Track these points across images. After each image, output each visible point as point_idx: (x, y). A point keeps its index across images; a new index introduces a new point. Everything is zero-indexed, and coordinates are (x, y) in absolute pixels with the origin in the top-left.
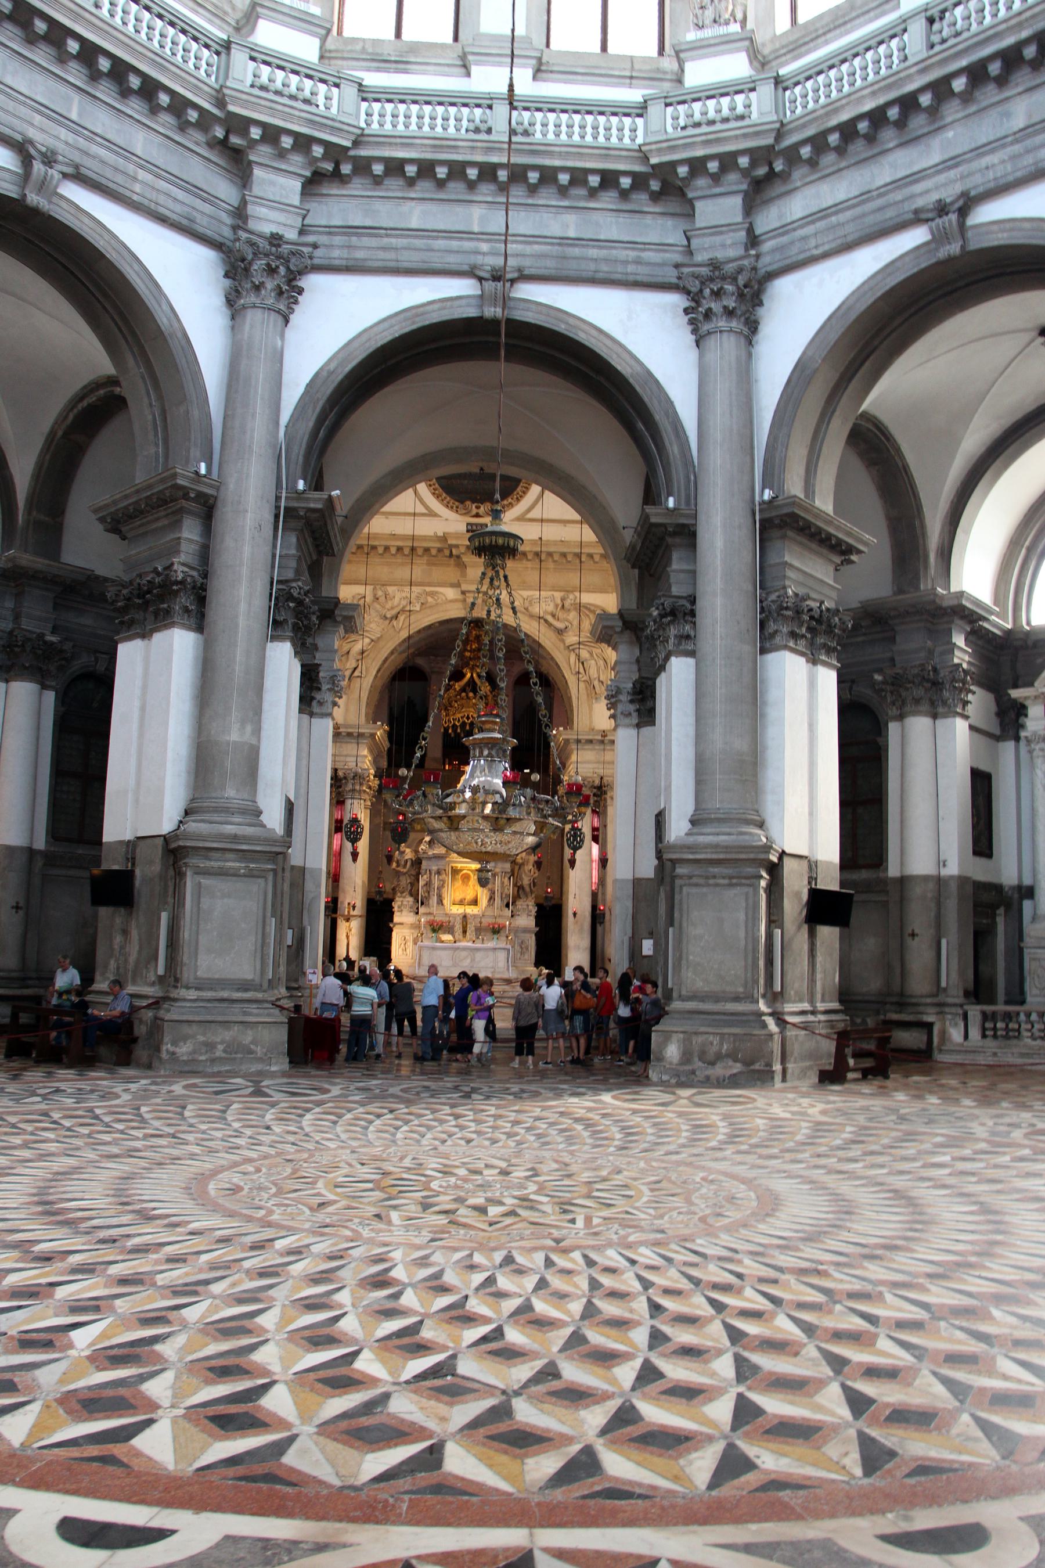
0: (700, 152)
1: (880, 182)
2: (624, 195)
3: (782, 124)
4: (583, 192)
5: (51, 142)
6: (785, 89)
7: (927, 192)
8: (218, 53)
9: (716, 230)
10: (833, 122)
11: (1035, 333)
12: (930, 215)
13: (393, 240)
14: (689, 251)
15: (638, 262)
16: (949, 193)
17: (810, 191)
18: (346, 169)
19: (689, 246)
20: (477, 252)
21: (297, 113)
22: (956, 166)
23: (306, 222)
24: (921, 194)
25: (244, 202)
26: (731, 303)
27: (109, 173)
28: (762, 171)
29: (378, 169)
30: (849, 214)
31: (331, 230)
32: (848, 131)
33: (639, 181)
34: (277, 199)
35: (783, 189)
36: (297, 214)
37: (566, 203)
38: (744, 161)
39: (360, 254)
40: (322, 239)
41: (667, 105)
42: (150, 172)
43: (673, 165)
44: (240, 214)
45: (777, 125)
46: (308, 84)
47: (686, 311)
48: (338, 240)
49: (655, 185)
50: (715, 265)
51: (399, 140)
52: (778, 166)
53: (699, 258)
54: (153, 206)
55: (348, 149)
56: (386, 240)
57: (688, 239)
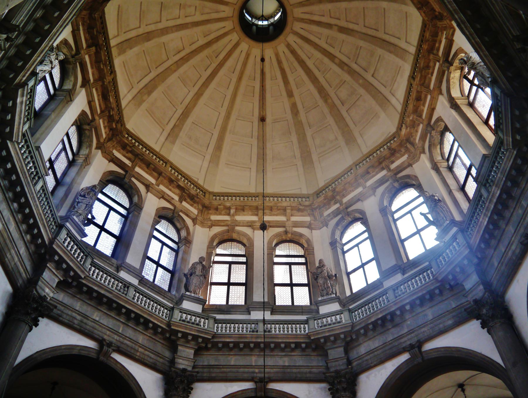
0: (327, 334)
1: (389, 339)
2: (303, 350)
3: (353, 323)
4: (289, 350)
5: (111, 339)
6: (352, 313)
7: (406, 341)
8: (170, 311)
9: (336, 360)
10: (370, 322)
11: (456, 387)
12: (409, 349)
13: (225, 369)
14: (327, 368)
15: (310, 372)
16: (414, 341)
17: (365, 344)
18: (209, 346)
19: (327, 366)
20: (254, 372)
21: (194, 328)
22: (413, 332)
23: (195, 364)
24: (404, 342)
25: (174, 359)
26: (345, 385)
27: (129, 349)
28: (349, 339)
29: (220, 345)
30: (380, 351)
31: (204, 367)
32: (375, 324)
33: (308, 345)
34: (185, 356)
35: (356, 344)
36: (192, 361)
37: (284, 354)
38: (342, 336)
39: (214, 375)
40: (201, 370)
41: (315, 320)
42: (143, 348)
43: (319, 339)
44: (172, 362)
45: (351, 324)
46: (198, 319)
47: (329, 389)
48: (206, 370)
49: (313, 346)
50: (337, 372)
51: (227, 336)
52: (354, 337)
53: (332, 370)
54: (142, 360)
55: (210, 339)
56: (223, 370)
57: (327, 364)
